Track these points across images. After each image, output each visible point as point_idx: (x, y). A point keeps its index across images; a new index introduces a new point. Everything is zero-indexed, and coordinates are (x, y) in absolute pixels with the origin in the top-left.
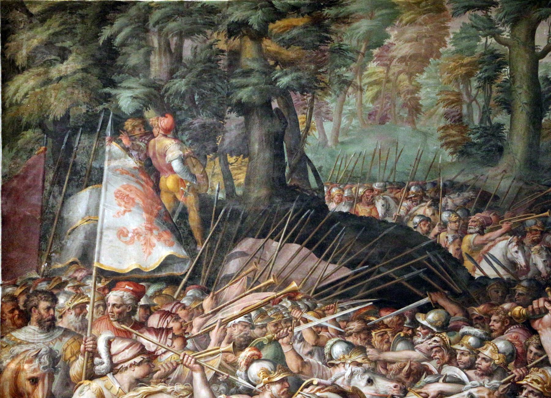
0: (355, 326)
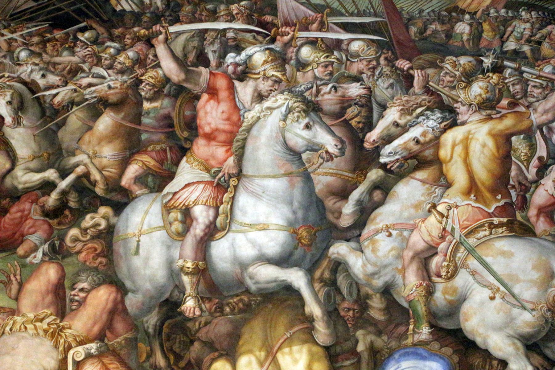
0: (36, 39)
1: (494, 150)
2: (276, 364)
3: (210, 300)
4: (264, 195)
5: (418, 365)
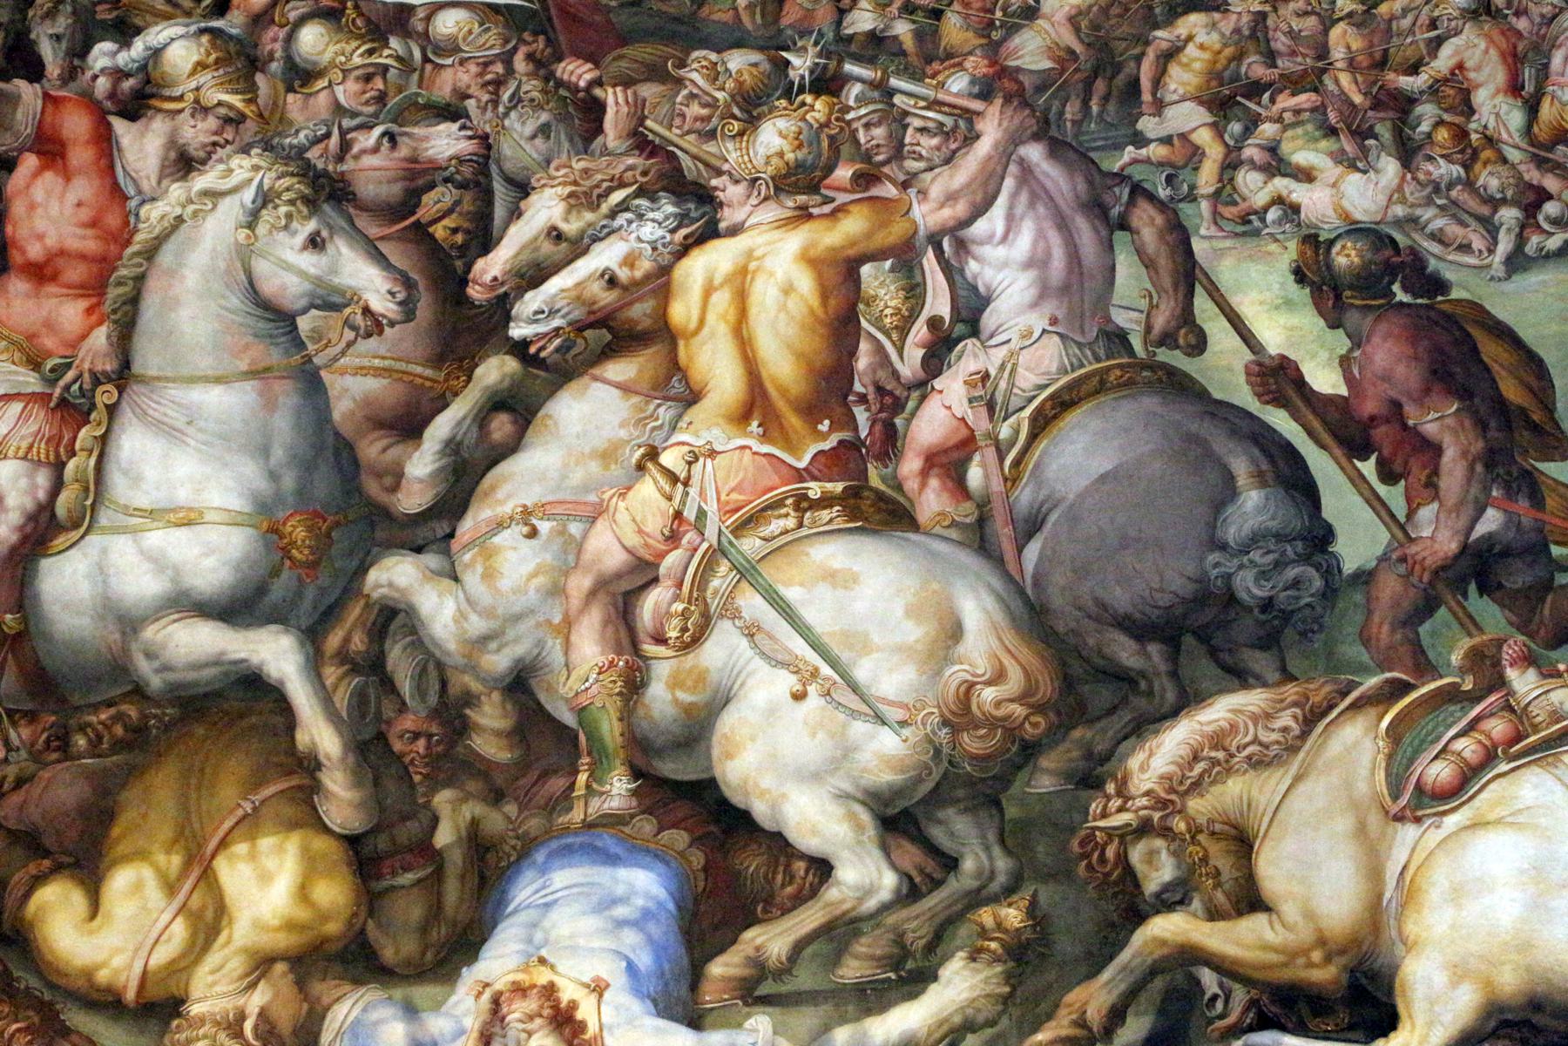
1: (815, 302)
2: (209, 885)
3: (32, 717)
4: (191, 430)
5: (596, 879)
